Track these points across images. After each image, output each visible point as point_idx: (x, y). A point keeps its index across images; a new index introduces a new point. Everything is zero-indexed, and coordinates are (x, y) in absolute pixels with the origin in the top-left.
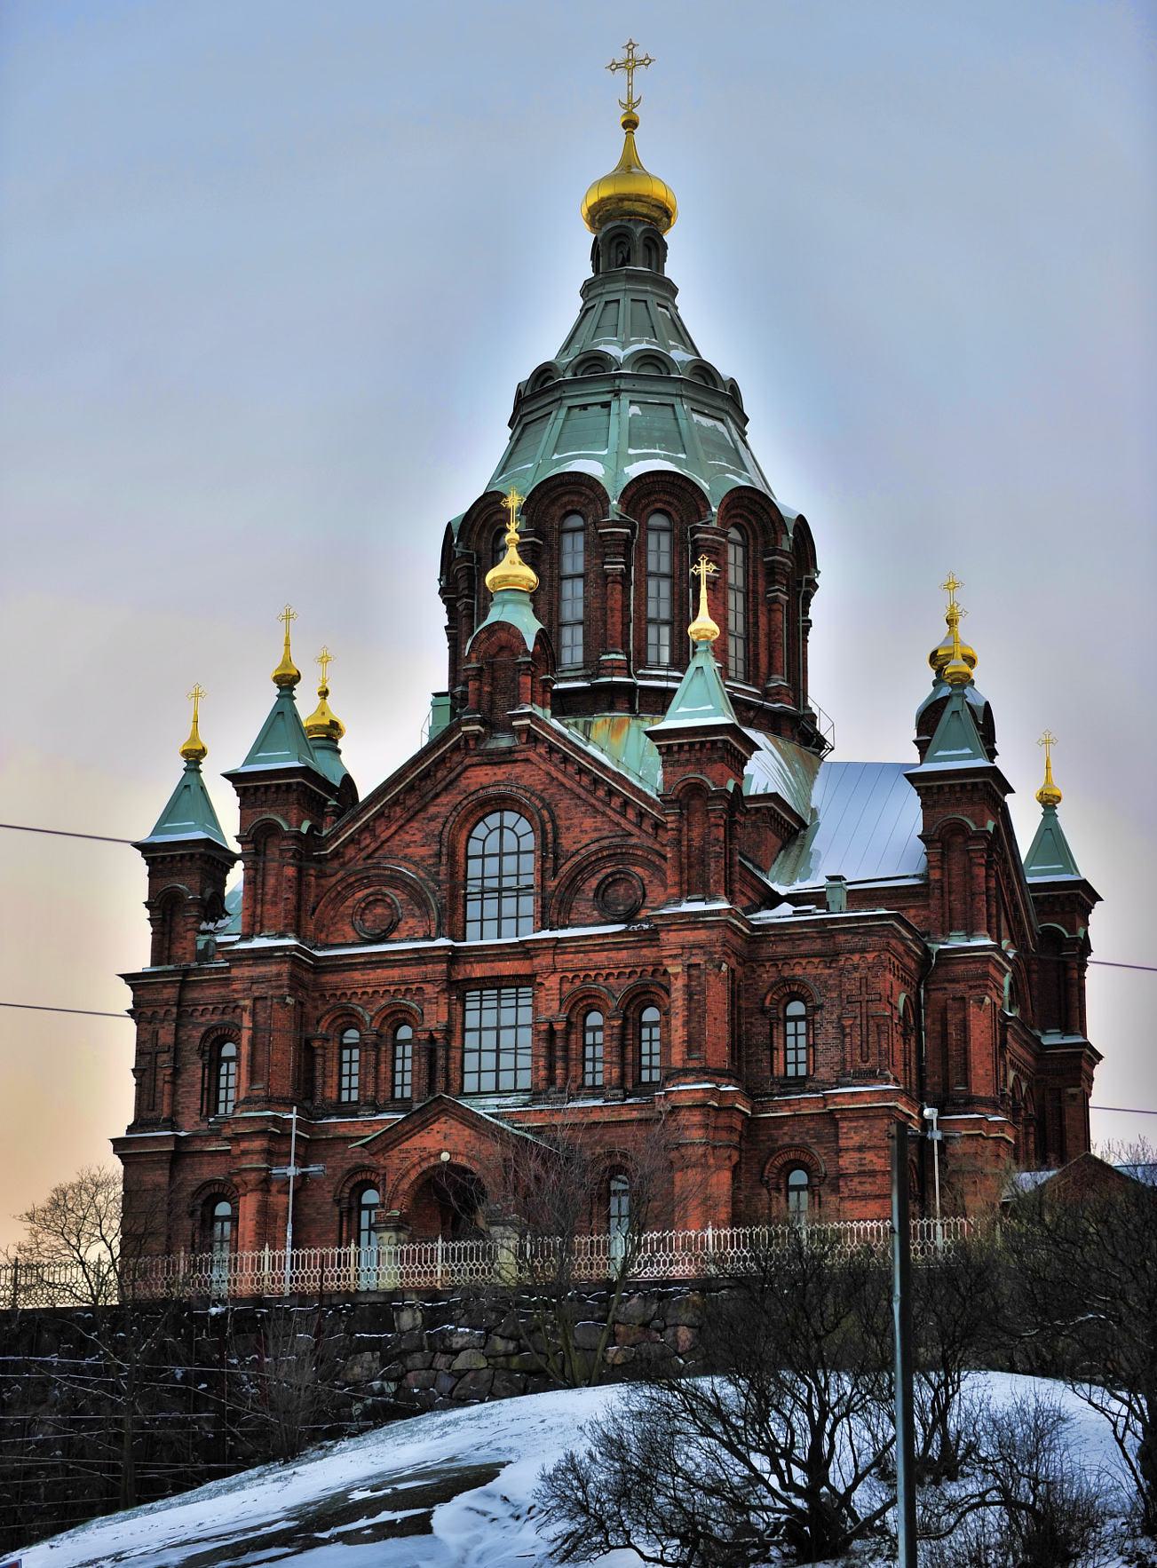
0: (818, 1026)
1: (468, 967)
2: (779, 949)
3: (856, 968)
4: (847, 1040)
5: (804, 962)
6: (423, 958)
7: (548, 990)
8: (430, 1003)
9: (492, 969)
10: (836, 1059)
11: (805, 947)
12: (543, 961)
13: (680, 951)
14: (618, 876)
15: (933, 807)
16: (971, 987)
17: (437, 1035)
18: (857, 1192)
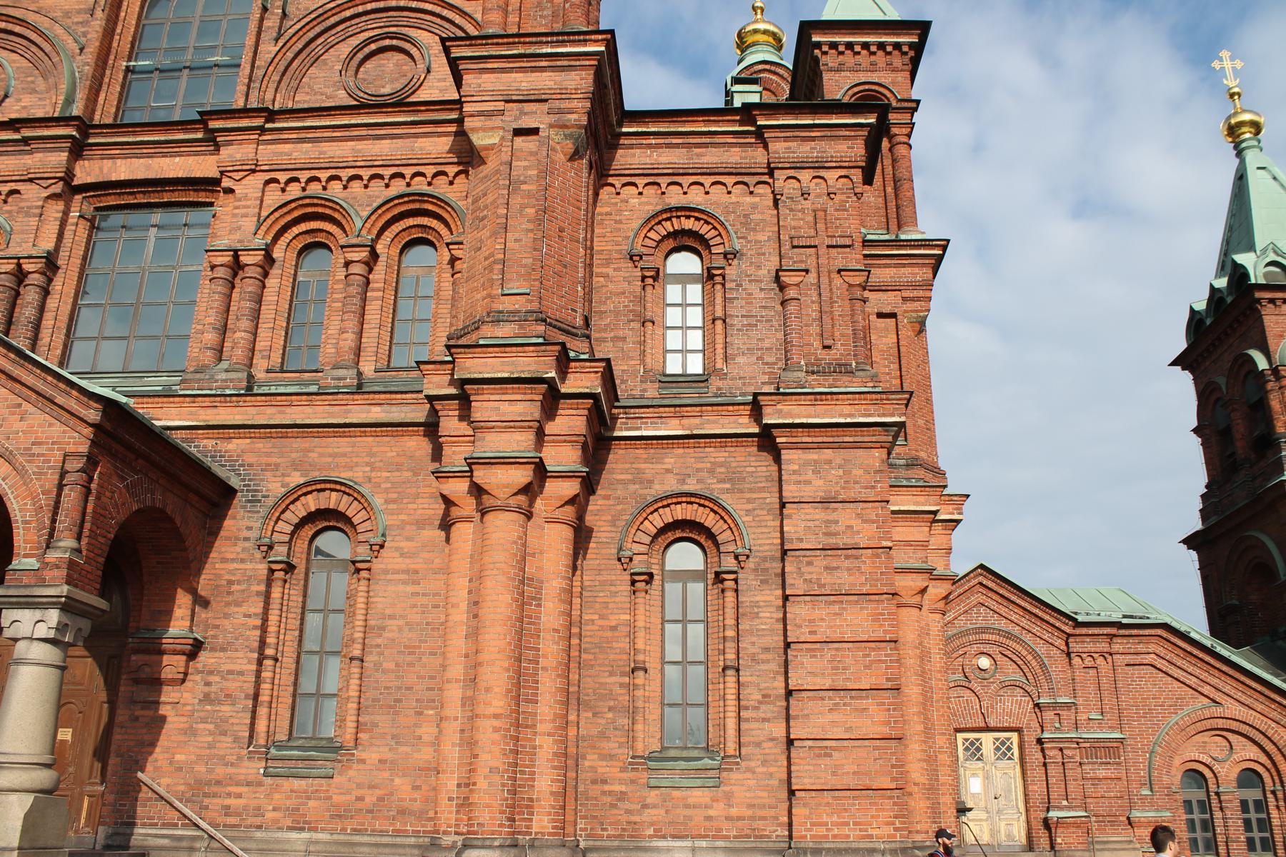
0: (733, 285)
1: (107, 164)
2: (664, 159)
3: (805, 194)
4: (792, 307)
5: (707, 181)
6: (25, 141)
7: (240, 200)
8: (28, 215)
9: (148, 167)
10: (767, 344)
11: (711, 157)
12: (236, 152)
13: (501, 106)
14: (387, 42)
15: (838, 70)
16: (905, 299)
17: (28, 267)
18: (821, 586)
